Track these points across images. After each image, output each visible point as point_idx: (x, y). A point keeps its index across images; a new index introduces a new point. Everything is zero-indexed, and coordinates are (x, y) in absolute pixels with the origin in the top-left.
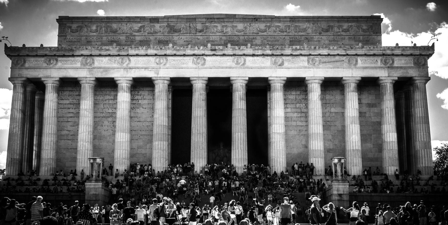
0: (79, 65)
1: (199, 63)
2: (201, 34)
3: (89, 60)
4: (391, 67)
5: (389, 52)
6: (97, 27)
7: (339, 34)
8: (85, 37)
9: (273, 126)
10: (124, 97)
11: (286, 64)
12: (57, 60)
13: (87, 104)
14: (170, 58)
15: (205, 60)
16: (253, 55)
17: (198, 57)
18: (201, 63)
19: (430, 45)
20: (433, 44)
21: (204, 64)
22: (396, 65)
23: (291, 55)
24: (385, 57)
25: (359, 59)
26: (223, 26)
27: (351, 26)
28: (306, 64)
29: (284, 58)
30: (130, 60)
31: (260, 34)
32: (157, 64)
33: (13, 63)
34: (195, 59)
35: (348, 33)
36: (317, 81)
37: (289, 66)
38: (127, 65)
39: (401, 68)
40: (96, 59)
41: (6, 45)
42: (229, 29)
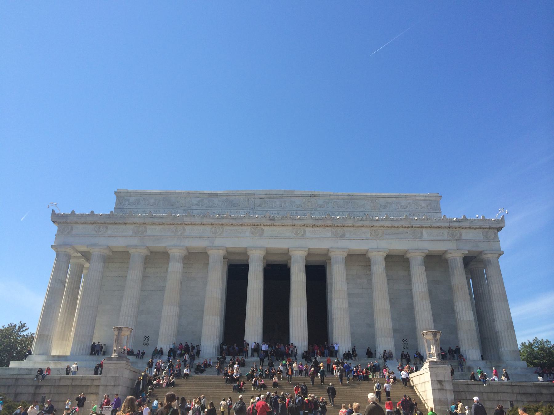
0: (130, 233)
2: (259, 208)
4: (459, 240)
5: (456, 224)
7: (398, 210)
8: (142, 210)
9: (336, 300)
11: (347, 235)
12: (107, 228)
14: (226, 228)
15: (263, 230)
16: (314, 226)
17: (255, 227)
23: (353, 226)
24: (451, 229)
25: (424, 231)
27: (409, 203)
28: (368, 235)
29: (345, 229)
30: (184, 229)
31: (319, 209)
32: (213, 233)
33: (59, 230)
34: (252, 229)
36: (381, 253)
39: (470, 241)
40: (149, 227)
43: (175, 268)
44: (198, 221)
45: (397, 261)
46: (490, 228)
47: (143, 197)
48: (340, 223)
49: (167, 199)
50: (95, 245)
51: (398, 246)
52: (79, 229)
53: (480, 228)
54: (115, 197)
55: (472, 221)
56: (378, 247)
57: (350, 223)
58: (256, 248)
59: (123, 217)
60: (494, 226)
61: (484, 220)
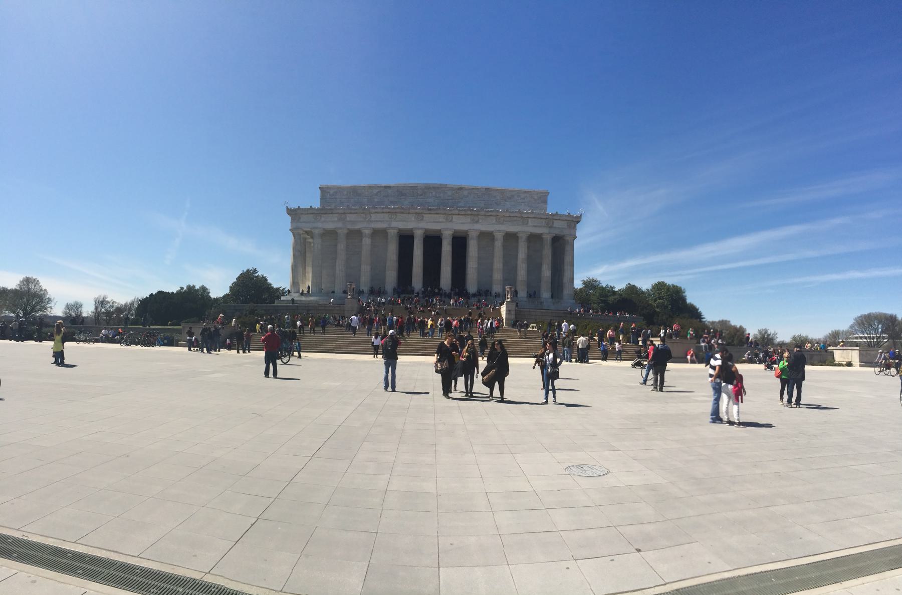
4: (551, 227)
13: (341, 246)
43: (367, 241)
44: (380, 211)
45: (511, 238)
47: (339, 190)
48: (476, 213)
49: (355, 191)
50: (317, 228)
51: (512, 229)
52: (304, 218)
55: (561, 216)
56: (499, 229)
57: (483, 213)
58: (419, 229)
59: (331, 209)
61: (569, 215)
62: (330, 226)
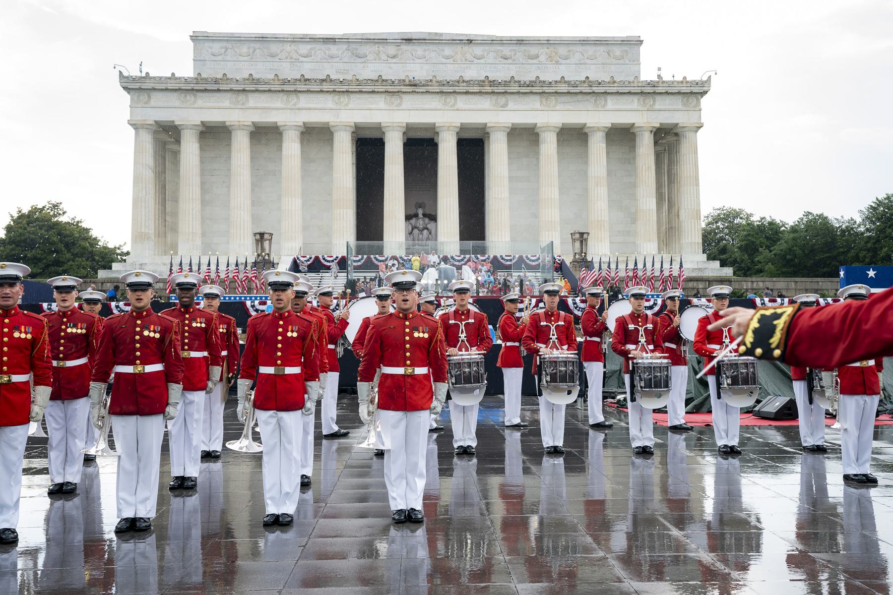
1: (393, 103)
2: (394, 60)
3: (242, 97)
5: (649, 90)
6: (249, 48)
10: (292, 147)
11: (511, 105)
14: (354, 97)
16: (467, 93)
18: (396, 103)
19: (705, 78)
20: (710, 77)
21: (400, 105)
22: (657, 107)
25: (610, 99)
26: (425, 51)
28: (537, 105)
30: (298, 98)
31: (476, 61)
33: (132, 100)
35: (594, 61)
37: (516, 107)
38: (294, 105)
41: (120, 72)
42: (433, 54)
45: (574, 137)
46: (692, 93)
53: (679, 93)
54: (192, 44)
60: (696, 89)
62: (214, 117)
